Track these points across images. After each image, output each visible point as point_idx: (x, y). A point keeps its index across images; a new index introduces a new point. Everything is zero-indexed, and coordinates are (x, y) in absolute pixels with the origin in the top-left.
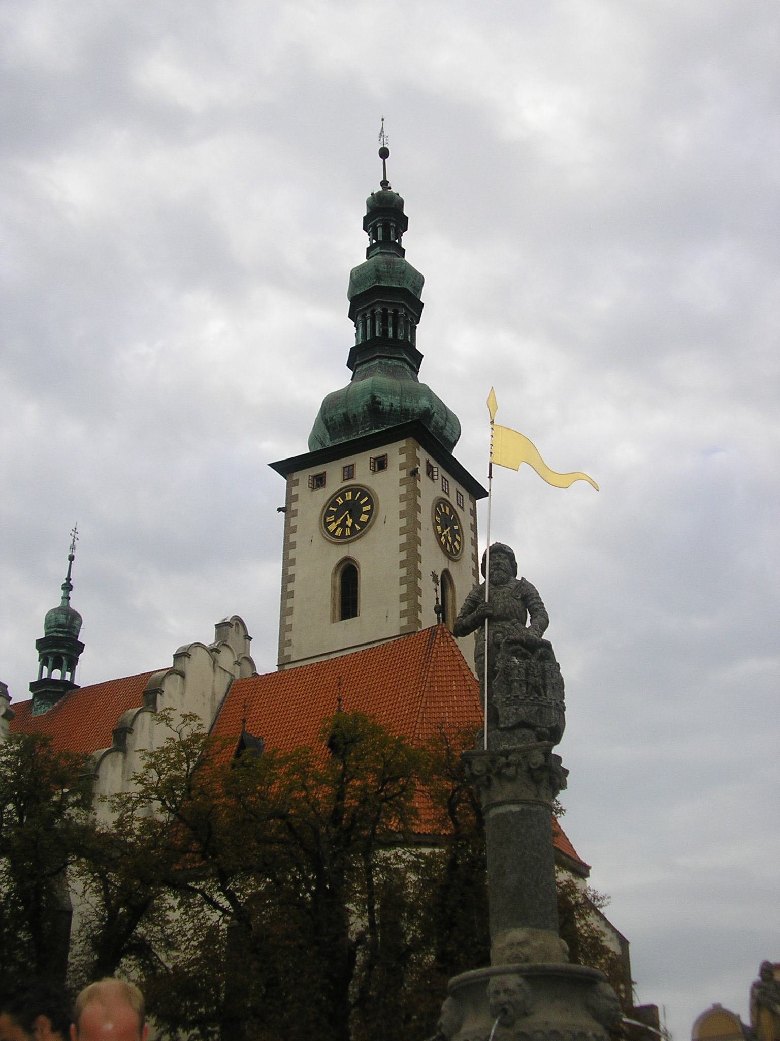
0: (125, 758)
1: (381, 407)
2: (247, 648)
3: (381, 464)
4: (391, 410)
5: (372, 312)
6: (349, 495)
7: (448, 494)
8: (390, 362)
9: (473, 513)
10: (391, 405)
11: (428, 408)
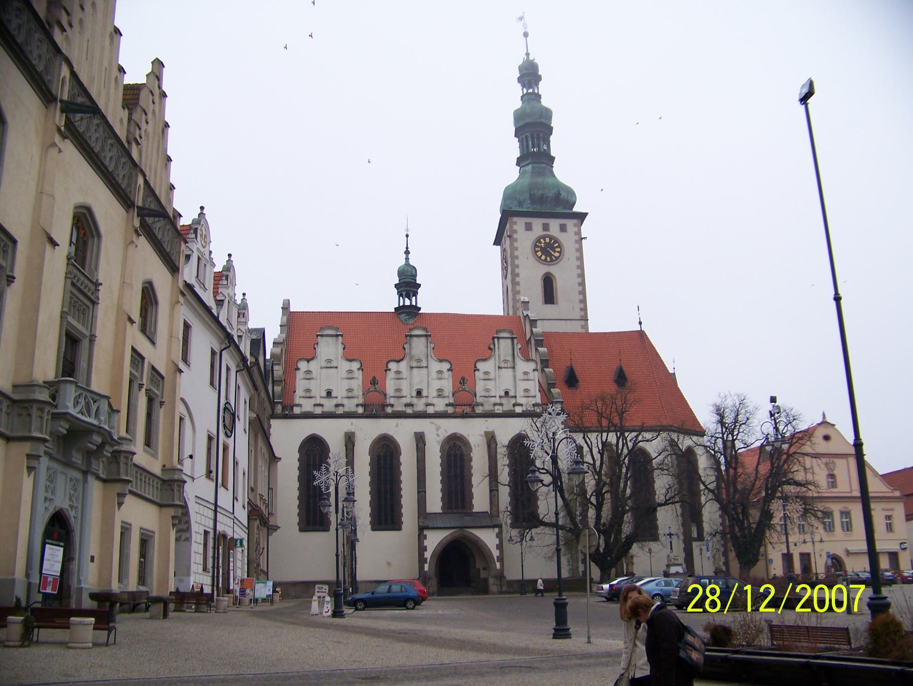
3: (563, 228)
5: (538, 135)
6: (548, 240)
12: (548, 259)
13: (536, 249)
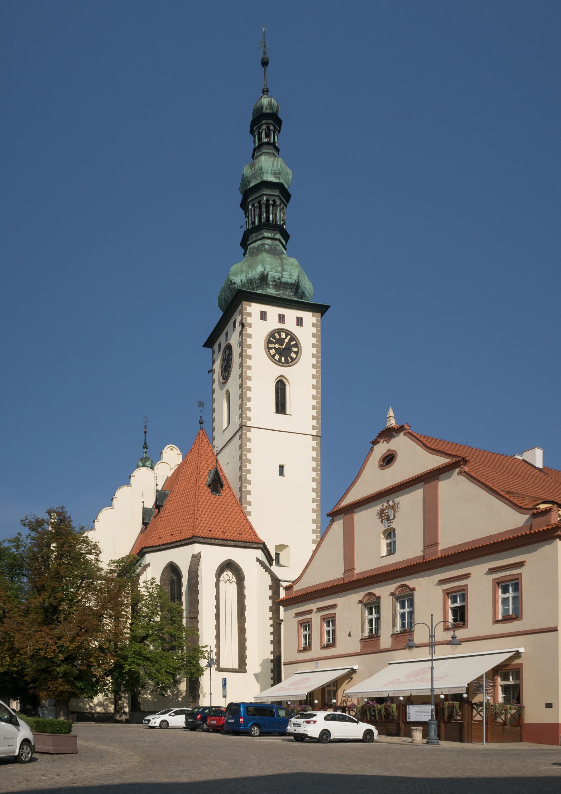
1: (236, 285)
4: (242, 285)
10: (241, 281)
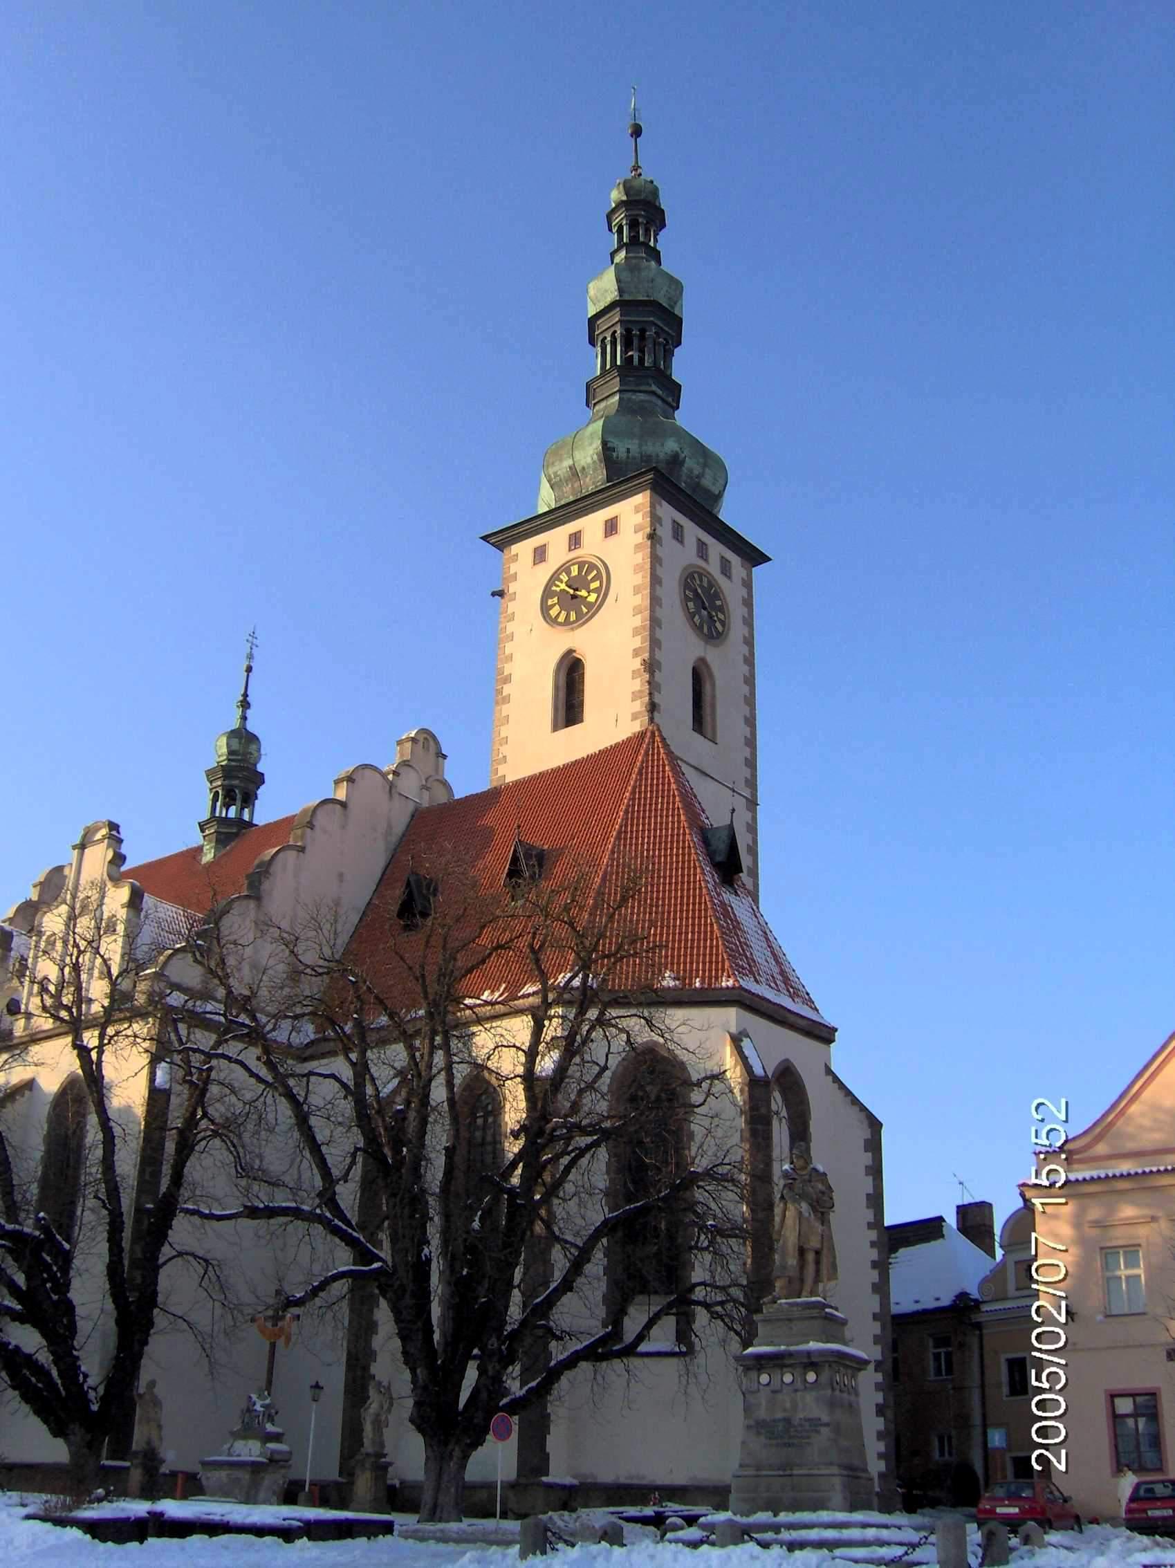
0: (259, 906)
1: (615, 454)
2: (438, 769)
3: (611, 527)
4: (628, 457)
6: (575, 571)
7: (706, 560)
8: (634, 397)
9: (748, 584)
11: (677, 452)
12: (573, 617)
13: (550, 602)
